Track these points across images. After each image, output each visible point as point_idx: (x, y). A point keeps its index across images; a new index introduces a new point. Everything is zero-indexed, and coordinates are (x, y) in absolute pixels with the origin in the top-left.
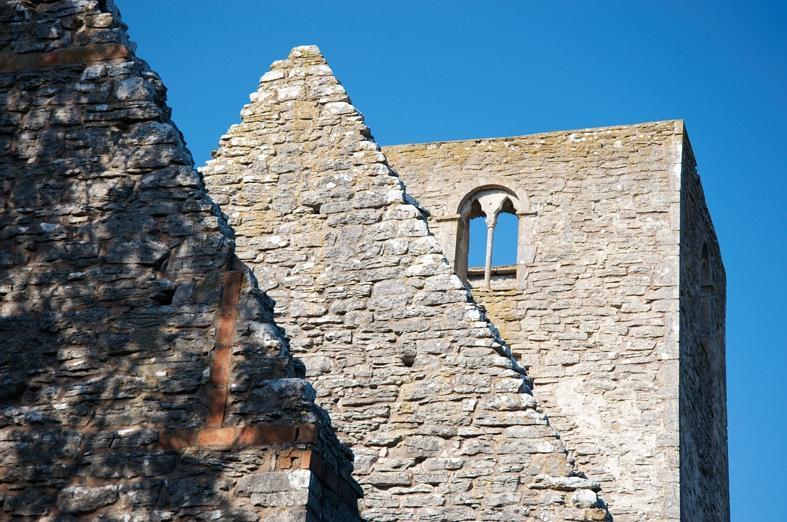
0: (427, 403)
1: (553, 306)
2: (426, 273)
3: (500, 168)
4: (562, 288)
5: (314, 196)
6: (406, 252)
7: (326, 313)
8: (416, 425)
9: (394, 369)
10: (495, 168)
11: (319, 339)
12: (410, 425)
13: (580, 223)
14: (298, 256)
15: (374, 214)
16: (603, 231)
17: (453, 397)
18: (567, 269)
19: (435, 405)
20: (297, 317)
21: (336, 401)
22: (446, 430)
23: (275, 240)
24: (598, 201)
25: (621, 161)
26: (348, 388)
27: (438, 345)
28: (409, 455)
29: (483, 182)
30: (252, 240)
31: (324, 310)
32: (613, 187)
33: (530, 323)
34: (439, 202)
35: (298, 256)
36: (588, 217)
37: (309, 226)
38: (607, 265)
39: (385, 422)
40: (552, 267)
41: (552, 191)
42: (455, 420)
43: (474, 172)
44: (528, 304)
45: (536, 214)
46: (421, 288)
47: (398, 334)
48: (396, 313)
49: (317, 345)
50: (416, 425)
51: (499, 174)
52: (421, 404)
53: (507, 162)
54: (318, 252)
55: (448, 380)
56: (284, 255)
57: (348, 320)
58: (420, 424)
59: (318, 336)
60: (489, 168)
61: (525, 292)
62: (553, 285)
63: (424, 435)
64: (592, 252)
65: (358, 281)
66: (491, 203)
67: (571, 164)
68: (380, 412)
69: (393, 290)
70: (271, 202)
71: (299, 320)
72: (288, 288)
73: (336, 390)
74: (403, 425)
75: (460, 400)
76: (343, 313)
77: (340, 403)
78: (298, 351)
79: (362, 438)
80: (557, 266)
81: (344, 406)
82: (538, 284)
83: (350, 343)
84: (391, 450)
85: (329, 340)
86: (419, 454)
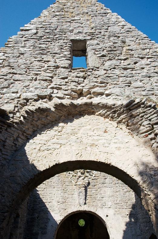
0: (134, 50)
2: (124, 25)
5: (86, 11)
6: (117, 21)
7: (95, 32)
8: (132, 55)
9: (120, 44)
11: (94, 37)
12: (130, 55)
14: (84, 21)
15: (104, 15)
17: (142, 49)
19: (136, 51)
20: (87, 33)
21: (104, 50)
22: (141, 56)
23: (76, 18)
26: (106, 47)
27: (133, 39)
28: (132, 62)
30: (69, 18)
31: (94, 31)
35: (84, 21)
37: (86, 16)
39: (121, 55)
42: (144, 54)
46: (123, 28)
47: (119, 37)
48: (117, 32)
49: (94, 39)
50: (132, 55)
52: (131, 51)
54: (90, 21)
55: (138, 46)
56: (79, 21)
57: (102, 34)
58: (133, 55)
59: (94, 37)
63: (135, 57)
65: (104, 26)
68: (119, 52)
69: (115, 28)
70: (73, 12)
71: (87, 33)
72: (82, 27)
73: (103, 48)
74: (128, 55)
75: (144, 50)
76: (101, 33)
77: (105, 51)
78: (88, 40)
79: (114, 58)
81: (106, 51)
83: (105, 38)
84: (125, 61)
85: (97, 38)
86: (136, 61)
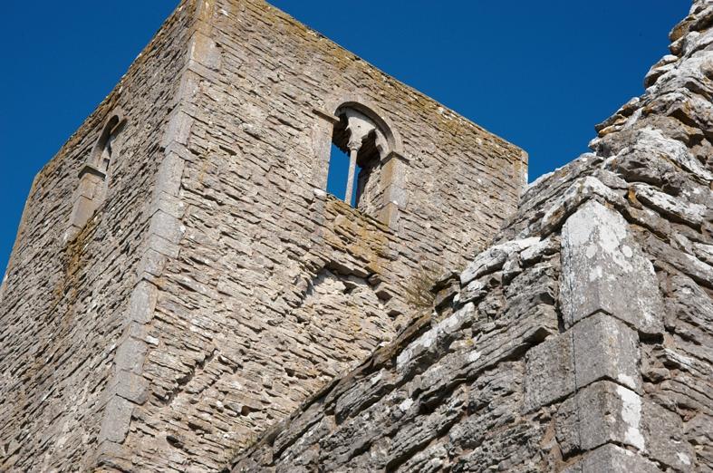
1: (423, 262)
3: (377, 97)
4: (431, 249)
10: (372, 94)
13: (447, 193)
16: (467, 214)
18: (437, 233)
24: (462, 183)
25: (480, 158)
29: (360, 101)
32: (475, 177)
33: (399, 267)
34: (315, 93)
36: (454, 193)
38: (468, 249)
40: (422, 223)
41: (424, 149)
43: (352, 85)
44: (401, 248)
45: (407, 161)
51: (375, 103)
53: (383, 96)
60: (365, 90)
61: (396, 234)
62: (423, 242)
64: (458, 229)
66: (359, 128)
67: (441, 134)
80: (428, 225)
82: (410, 232)
